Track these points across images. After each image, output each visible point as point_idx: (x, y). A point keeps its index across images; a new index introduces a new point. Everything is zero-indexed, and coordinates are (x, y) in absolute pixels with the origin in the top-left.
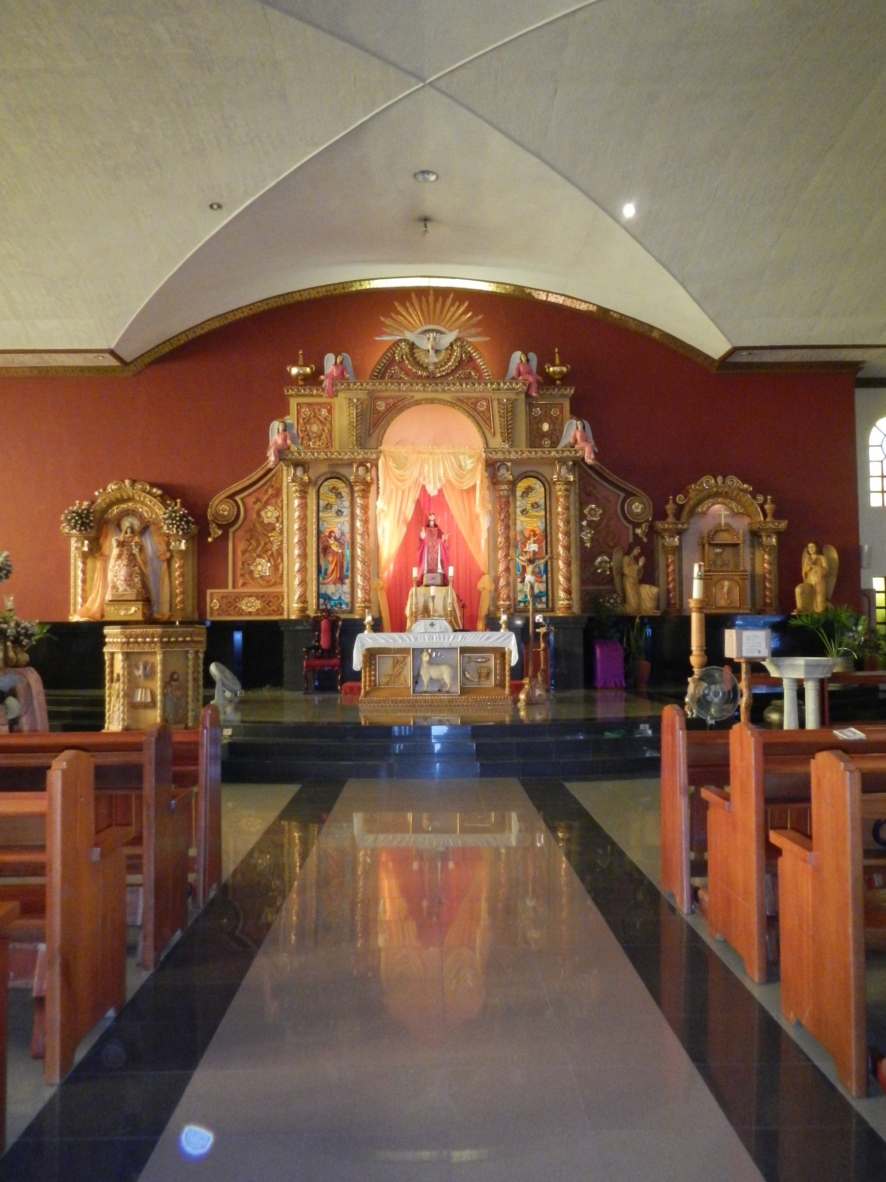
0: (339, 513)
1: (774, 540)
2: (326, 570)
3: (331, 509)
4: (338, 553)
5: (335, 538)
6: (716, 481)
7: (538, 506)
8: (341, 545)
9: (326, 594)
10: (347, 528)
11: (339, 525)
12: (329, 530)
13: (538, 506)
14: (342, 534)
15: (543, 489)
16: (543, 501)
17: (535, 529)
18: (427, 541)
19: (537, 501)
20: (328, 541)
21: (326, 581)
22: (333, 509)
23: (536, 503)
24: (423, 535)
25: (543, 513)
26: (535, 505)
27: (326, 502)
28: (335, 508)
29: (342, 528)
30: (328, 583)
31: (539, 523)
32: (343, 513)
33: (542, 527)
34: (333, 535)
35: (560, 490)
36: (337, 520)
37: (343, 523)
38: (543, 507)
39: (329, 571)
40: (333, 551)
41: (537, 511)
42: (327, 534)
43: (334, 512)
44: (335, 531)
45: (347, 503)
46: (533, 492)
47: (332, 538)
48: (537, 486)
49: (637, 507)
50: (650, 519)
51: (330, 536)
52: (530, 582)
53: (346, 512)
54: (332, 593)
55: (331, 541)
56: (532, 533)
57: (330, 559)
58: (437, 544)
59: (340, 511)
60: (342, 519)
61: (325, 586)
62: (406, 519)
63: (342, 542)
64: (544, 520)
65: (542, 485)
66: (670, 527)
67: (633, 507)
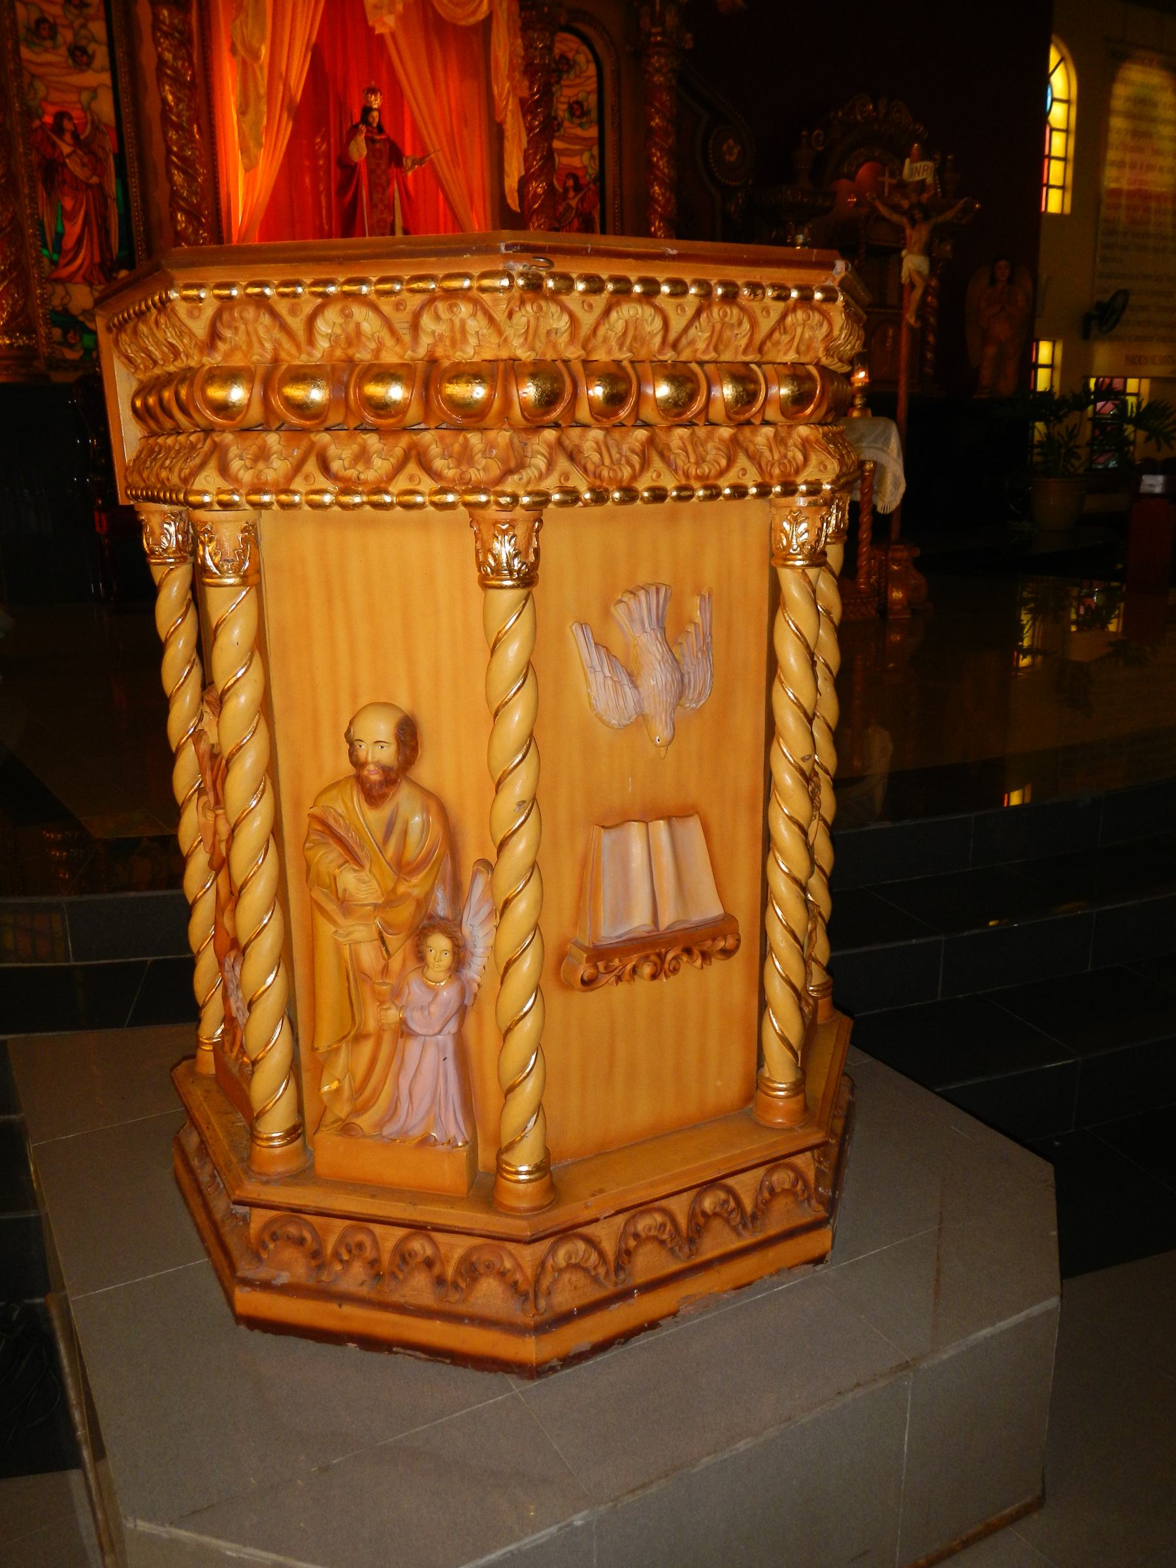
0: (80, 56)
1: (948, 248)
2: (59, 237)
3: (53, 37)
4: (88, 186)
5: (75, 135)
6: (875, 108)
7: (585, 113)
8: (96, 165)
9: (66, 312)
10: (105, 108)
11: (85, 97)
12: (52, 109)
13: (585, 113)
14: (96, 127)
15: (592, 70)
16: (593, 99)
17: (580, 174)
18: (364, 171)
19: (582, 96)
20: (54, 145)
21: (65, 272)
22: (60, 39)
23: (579, 103)
24: (359, 149)
25: (593, 132)
26: (577, 109)
27: (35, 15)
28: (66, 36)
29: (94, 105)
30: (70, 279)
31: (586, 155)
32: (91, 58)
33: (593, 171)
34: (67, 125)
35: (658, 71)
36: (76, 79)
37: (94, 91)
38: (594, 115)
39: (69, 243)
40: (76, 178)
41: (581, 125)
42: (48, 119)
43: (63, 51)
44: (74, 114)
45: (98, 28)
46: (572, 75)
47: (68, 137)
48: (581, 58)
49: (732, 152)
50: (750, 182)
51: (58, 129)
52: (919, 273)
53: (101, 55)
54: (85, 312)
55: (66, 149)
56: (570, 183)
57: (68, 203)
58: (389, 182)
59: (84, 51)
60: (90, 78)
61: (60, 290)
62: (292, 99)
63: (101, 154)
64: (595, 151)
65: (590, 57)
66: (806, 200)
67: (725, 148)
